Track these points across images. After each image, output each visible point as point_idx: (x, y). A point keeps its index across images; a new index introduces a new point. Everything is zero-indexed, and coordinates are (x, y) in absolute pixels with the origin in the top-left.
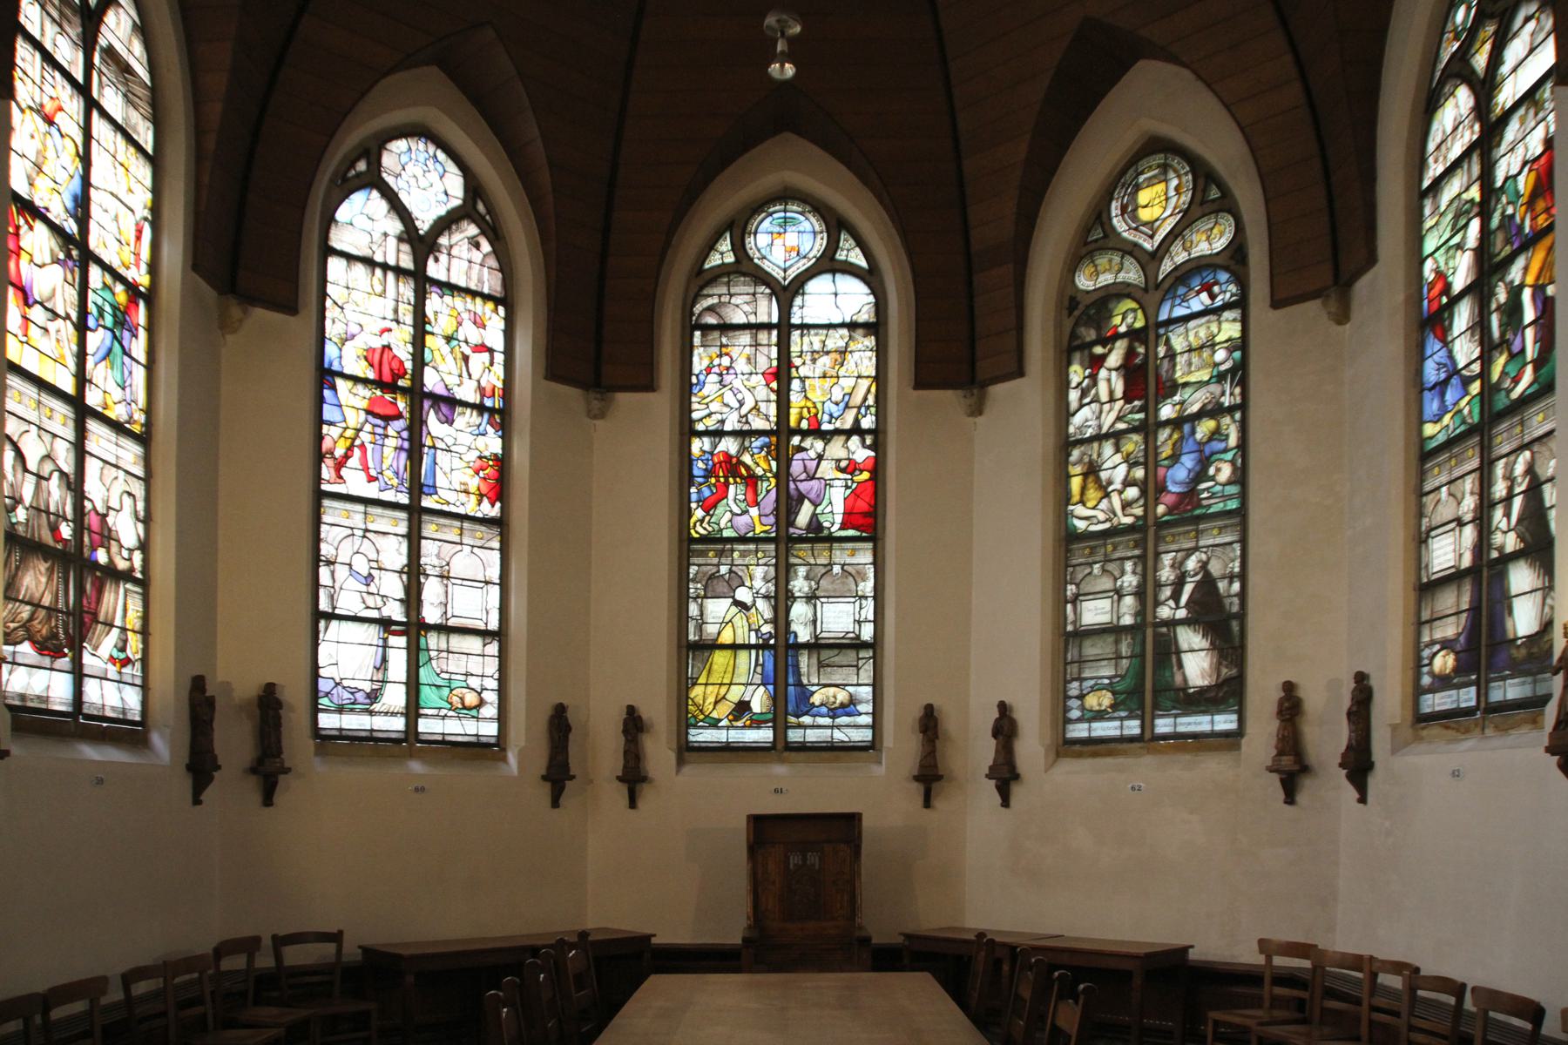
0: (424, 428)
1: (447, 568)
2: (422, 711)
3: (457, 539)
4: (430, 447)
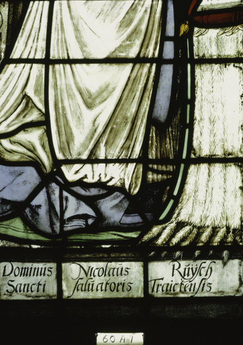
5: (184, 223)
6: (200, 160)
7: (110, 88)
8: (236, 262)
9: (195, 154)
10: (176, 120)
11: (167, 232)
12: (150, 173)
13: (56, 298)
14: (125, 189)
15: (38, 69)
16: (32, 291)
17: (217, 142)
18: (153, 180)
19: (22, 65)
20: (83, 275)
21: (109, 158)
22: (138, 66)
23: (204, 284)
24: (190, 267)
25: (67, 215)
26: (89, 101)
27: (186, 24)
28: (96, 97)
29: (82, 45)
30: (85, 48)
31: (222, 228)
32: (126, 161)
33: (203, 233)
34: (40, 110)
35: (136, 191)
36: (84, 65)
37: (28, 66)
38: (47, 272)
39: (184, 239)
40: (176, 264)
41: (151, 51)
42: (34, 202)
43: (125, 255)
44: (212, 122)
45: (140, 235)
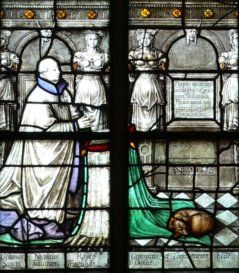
1: (164, 60)
6: (90, 209)
7: (50, 177)
8: (106, 253)
9: (88, 206)
10: (80, 192)
11: (75, 239)
12: (68, 214)
13: (24, 269)
14: (57, 221)
15: (18, 169)
16: (14, 266)
17: (98, 200)
18: (69, 217)
19: (11, 167)
20: (37, 259)
21: (49, 207)
22: (63, 168)
23: (92, 263)
24: (86, 255)
25: (30, 233)
26: (41, 183)
27: (84, 150)
28: (44, 181)
29: (38, 159)
30: (39, 161)
31: (100, 238)
33: (91, 240)
35: (61, 222)
36: (39, 168)
37: (14, 168)
38: (21, 258)
39: (82, 243)
40: (79, 254)
41: (69, 162)
42: (15, 227)
43: (56, 250)
45: (63, 241)
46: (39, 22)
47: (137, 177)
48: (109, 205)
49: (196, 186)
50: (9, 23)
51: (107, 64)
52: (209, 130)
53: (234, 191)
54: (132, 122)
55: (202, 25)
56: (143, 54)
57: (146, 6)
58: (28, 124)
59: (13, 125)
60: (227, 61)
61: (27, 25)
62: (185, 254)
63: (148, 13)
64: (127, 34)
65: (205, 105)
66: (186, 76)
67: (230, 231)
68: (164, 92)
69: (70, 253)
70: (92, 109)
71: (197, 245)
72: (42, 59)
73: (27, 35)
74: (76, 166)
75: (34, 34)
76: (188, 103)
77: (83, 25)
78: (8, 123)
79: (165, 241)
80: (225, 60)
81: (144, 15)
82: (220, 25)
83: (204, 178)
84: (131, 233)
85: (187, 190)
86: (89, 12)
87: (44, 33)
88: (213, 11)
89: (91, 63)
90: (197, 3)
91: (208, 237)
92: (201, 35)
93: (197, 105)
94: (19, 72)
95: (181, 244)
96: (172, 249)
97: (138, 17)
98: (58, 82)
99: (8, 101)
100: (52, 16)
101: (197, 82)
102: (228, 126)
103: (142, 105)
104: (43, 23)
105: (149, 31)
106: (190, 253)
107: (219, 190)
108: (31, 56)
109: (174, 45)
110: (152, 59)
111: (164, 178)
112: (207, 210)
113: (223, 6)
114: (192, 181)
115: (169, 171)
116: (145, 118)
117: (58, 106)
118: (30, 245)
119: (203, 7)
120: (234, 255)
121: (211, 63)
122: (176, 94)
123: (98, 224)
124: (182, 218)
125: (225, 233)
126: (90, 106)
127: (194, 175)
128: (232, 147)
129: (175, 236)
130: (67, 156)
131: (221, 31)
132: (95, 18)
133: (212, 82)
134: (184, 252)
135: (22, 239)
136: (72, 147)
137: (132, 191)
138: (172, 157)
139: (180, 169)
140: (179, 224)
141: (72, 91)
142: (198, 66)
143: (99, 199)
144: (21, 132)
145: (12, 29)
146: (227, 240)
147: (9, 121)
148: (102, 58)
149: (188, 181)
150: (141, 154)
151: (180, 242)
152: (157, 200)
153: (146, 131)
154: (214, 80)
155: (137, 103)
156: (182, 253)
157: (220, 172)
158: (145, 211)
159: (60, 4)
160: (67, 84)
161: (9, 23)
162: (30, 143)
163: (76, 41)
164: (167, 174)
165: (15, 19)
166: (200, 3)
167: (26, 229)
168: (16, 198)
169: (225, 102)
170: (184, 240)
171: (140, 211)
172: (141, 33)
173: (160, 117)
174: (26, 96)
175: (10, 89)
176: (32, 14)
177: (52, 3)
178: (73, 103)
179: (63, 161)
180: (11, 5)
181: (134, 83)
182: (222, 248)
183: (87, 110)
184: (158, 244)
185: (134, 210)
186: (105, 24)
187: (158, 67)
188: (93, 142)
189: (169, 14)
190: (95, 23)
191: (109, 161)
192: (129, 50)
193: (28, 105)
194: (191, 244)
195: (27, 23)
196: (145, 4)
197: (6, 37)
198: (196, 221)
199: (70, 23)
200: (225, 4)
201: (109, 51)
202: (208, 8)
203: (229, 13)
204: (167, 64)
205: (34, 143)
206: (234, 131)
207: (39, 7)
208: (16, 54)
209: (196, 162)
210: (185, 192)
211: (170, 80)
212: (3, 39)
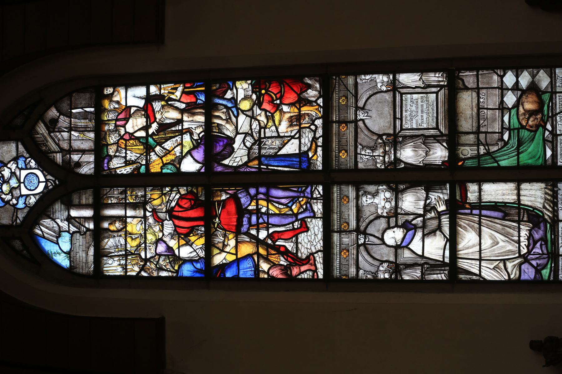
0: (242, 170)
1: (384, 137)
2: (549, 162)
3: (352, 126)
4: (260, 163)
5: (543, 206)
6: (519, 199)
8: (559, 185)
9: (516, 201)
10: (503, 209)
11: (547, 212)
15: (483, 263)
19: (482, 270)
22: (482, 224)
25: (541, 252)
26: (496, 243)
32: (519, 229)
34: (499, 263)
35: (531, 225)
36: (482, 245)
37: (482, 267)
39: (550, 206)
41: (476, 219)
42: (535, 265)
44: (504, 195)
46: (352, 246)
47: (490, 159)
48: (515, 183)
49: (497, 107)
50: (352, 271)
51: (388, 186)
52: (447, 97)
53: (501, 74)
54: (440, 164)
55: (354, 106)
56: (379, 156)
57: (337, 154)
58: (442, 255)
59: (443, 267)
60: (385, 84)
61: (354, 256)
62: (559, 115)
63: (343, 152)
64: (363, 170)
65: (424, 101)
66: (398, 119)
67: (537, 77)
68: (412, 137)
69: (560, 217)
70: (429, 199)
71: (551, 105)
72: (384, 243)
73: (363, 256)
74: (480, 212)
75: (362, 250)
76: (422, 116)
77: (354, 207)
78: (442, 272)
79: (547, 133)
80: (384, 85)
81: (345, 155)
82: (353, 90)
83: (489, 101)
84: (541, 163)
85: (500, 115)
86: (343, 202)
87: (361, 241)
88: (342, 97)
89: (387, 200)
90: (334, 111)
91: (543, 96)
92: (362, 106)
93: (424, 108)
94: (395, 263)
95: (550, 119)
96: (555, 127)
97: (347, 160)
98: (405, 229)
99: (422, 272)
100: (347, 234)
101: (404, 109)
102: (442, 81)
103: (425, 155)
104: (352, 242)
105: (359, 151)
106: (558, 111)
107: (500, 87)
108: (382, 253)
109: (371, 130)
110: (384, 148)
111: (490, 135)
112: (518, 97)
113: (337, 88)
114: (492, 111)
115: (483, 130)
116: (436, 153)
117: (426, 228)
118: (551, 253)
119: (338, 105)
120: (559, 72)
121: (387, 97)
122: (415, 127)
123: (532, 192)
124: (526, 118)
125: (539, 81)
126: (426, 200)
127: (487, 109)
128: (461, 77)
129: (543, 124)
130: (471, 220)
131: (359, 89)
132: (348, 197)
133: (404, 95)
134: (557, 117)
135: (546, 259)
136: (462, 216)
137: (503, 163)
138: (471, 128)
139: (481, 122)
140: (532, 121)
141: (412, 217)
142: (390, 109)
143: (510, 192)
144: (450, 260)
145: (358, 268)
146: (545, 79)
147: (440, 271)
148: (383, 191)
149: (493, 114)
150: (469, 156)
151: (548, 120)
152: (510, 141)
153: (448, 152)
154: (402, 94)
155: (423, 160)
156: (558, 118)
157: (484, 86)
158: (520, 151)
159: (336, 227)
160: (407, 221)
161: (352, 271)
162: (460, 252)
163: (368, 213)
164: (486, 133)
165: (349, 266)
166: (335, 108)
167: (538, 256)
168: (510, 265)
169: (421, 84)
170: (546, 116)
171: (520, 156)
172: (361, 157)
173: (435, 139)
174: (417, 256)
175: (411, 271)
176: (345, 251)
177: (335, 234)
178: (423, 216)
179: (475, 224)
180: (337, 269)
181: (405, 163)
182: (552, 84)
183: (430, 203)
184: (550, 139)
185: (520, 161)
186: (353, 189)
187: (390, 143)
188: (458, 198)
189: (344, 134)
190: (352, 198)
191: (475, 184)
192: (376, 168)
193: (426, 255)
194: (550, 111)
195: (352, 256)
196: (336, 155)
197: (365, 274)
198: (529, 106)
199: (352, 219)
200: (335, 87)
201: (377, 185)
202: (339, 101)
203: (343, 83)
204: (388, 135)
205: (459, 250)
206: (447, 75)
207: (338, 246)
208: (380, 265)
209: (476, 107)
210: (503, 116)
211: (402, 132)
212: (367, 277)
